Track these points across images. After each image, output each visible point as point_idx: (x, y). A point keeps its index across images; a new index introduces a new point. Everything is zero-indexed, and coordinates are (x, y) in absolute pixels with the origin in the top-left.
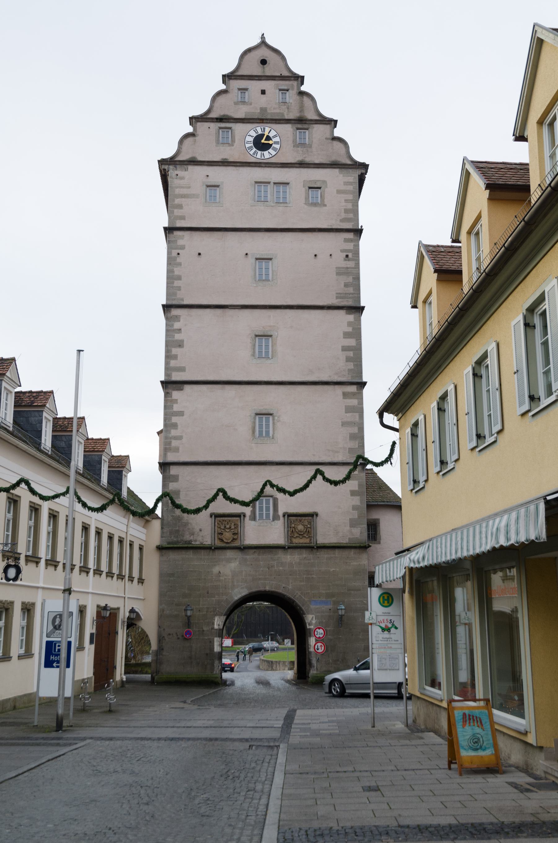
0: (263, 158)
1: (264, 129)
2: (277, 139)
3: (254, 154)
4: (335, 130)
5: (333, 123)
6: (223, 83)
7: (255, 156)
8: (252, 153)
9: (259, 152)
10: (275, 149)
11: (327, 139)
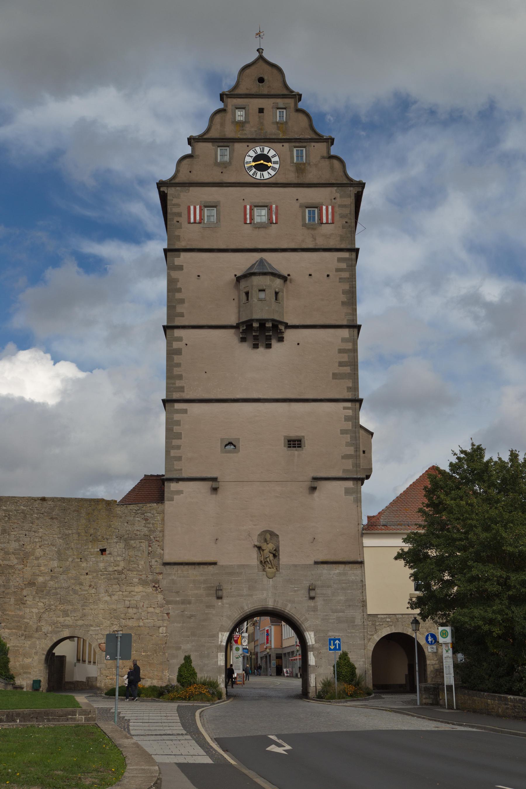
0: (262, 178)
1: (263, 149)
2: (276, 159)
3: (253, 174)
4: (332, 148)
5: (331, 141)
6: (221, 100)
7: (254, 177)
8: (251, 173)
9: (259, 173)
11: (323, 157)
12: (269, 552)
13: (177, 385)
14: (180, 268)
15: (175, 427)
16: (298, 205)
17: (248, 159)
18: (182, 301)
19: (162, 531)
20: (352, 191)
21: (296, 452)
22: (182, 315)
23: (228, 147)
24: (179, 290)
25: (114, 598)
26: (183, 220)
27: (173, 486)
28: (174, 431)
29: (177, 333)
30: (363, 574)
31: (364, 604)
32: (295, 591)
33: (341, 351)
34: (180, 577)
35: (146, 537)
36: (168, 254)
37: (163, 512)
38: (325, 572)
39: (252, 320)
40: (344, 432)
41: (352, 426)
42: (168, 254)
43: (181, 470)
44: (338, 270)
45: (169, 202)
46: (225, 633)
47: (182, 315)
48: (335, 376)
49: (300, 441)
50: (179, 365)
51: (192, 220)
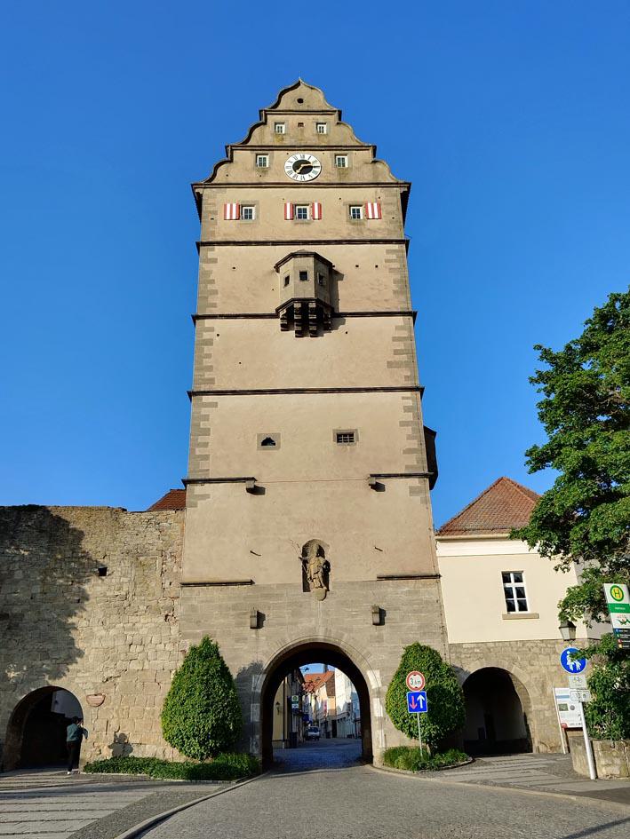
2: (318, 164)
8: (291, 176)
10: (315, 172)
12: (316, 567)
13: (206, 377)
14: (215, 261)
15: (201, 423)
16: (342, 204)
17: (287, 164)
18: (215, 292)
19: (181, 544)
20: (398, 191)
21: (348, 447)
22: (214, 305)
23: (267, 155)
24: (212, 282)
25: (112, 632)
26: (219, 217)
27: (198, 489)
28: (202, 426)
29: (208, 322)
30: (439, 589)
31: (444, 633)
32: (353, 616)
33: (394, 339)
34: (202, 602)
35: (162, 553)
36: (201, 248)
37: (183, 521)
38: (390, 590)
39: (293, 300)
40: (404, 424)
41: (414, 417)
42: (201, 248)
43: (208, 470)
44: (387, 261)
45: (204, 202)
46: (261, 676)
47: (214, 305)
48: (390, 364)
49: (352, 435)
50: (209, 356)
51: (228, 217)
